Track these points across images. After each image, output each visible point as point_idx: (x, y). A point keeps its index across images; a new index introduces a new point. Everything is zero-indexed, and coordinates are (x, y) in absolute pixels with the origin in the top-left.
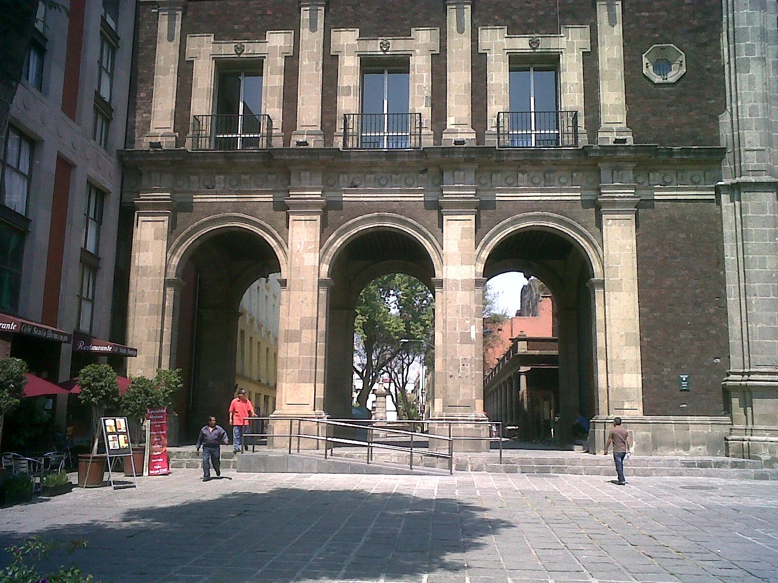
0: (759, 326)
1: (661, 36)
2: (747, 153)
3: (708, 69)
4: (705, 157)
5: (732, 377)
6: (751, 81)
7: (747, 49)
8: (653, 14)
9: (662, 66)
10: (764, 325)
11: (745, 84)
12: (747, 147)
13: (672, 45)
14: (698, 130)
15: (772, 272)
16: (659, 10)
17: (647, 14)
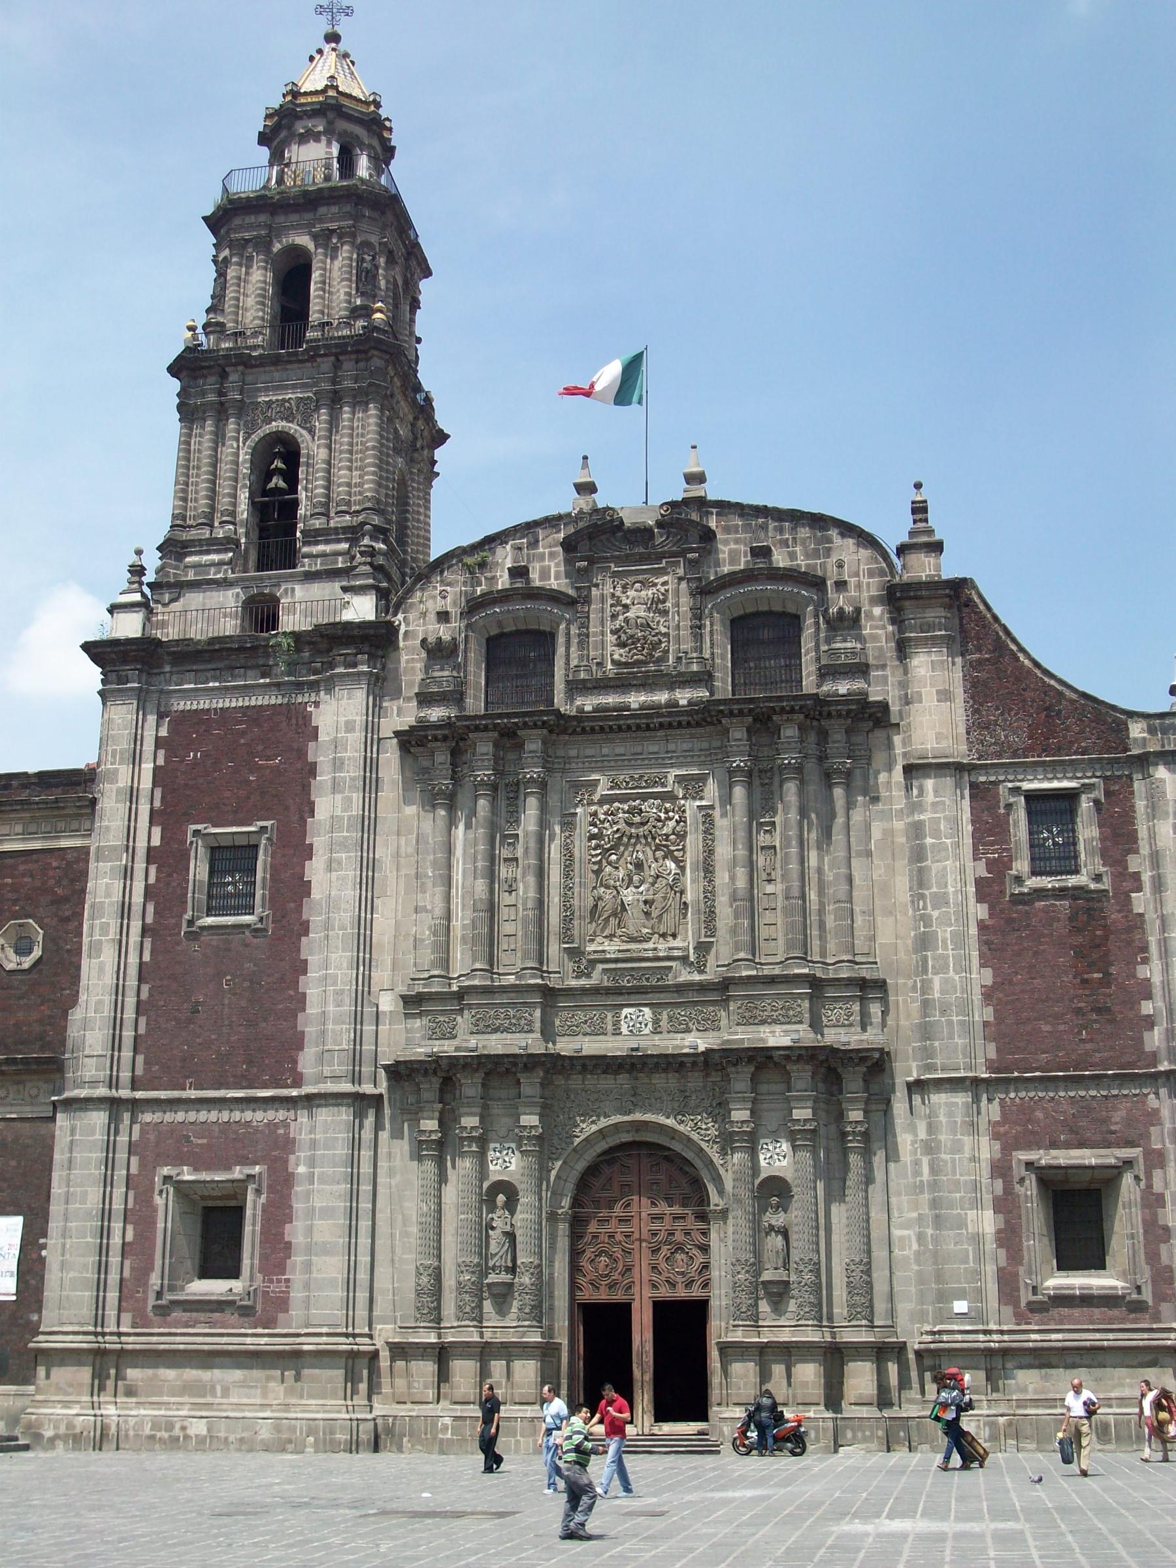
0: (71, 1275)
1: (22, 908)
2: (87, 1059)
3: (68, 951)
4: (34, 1067)
5: (41, 1338)
6: (101, 969)
7: (101, 929)
8: (16, 881)
9: (23, 949)
10: (76, 1274)
11: (94, 973)
12: (86, 1053)
13: (31, 921)
14: (48, 1028)
15: (92, 1209)
16: (23, 875)
17: (9, 881)
